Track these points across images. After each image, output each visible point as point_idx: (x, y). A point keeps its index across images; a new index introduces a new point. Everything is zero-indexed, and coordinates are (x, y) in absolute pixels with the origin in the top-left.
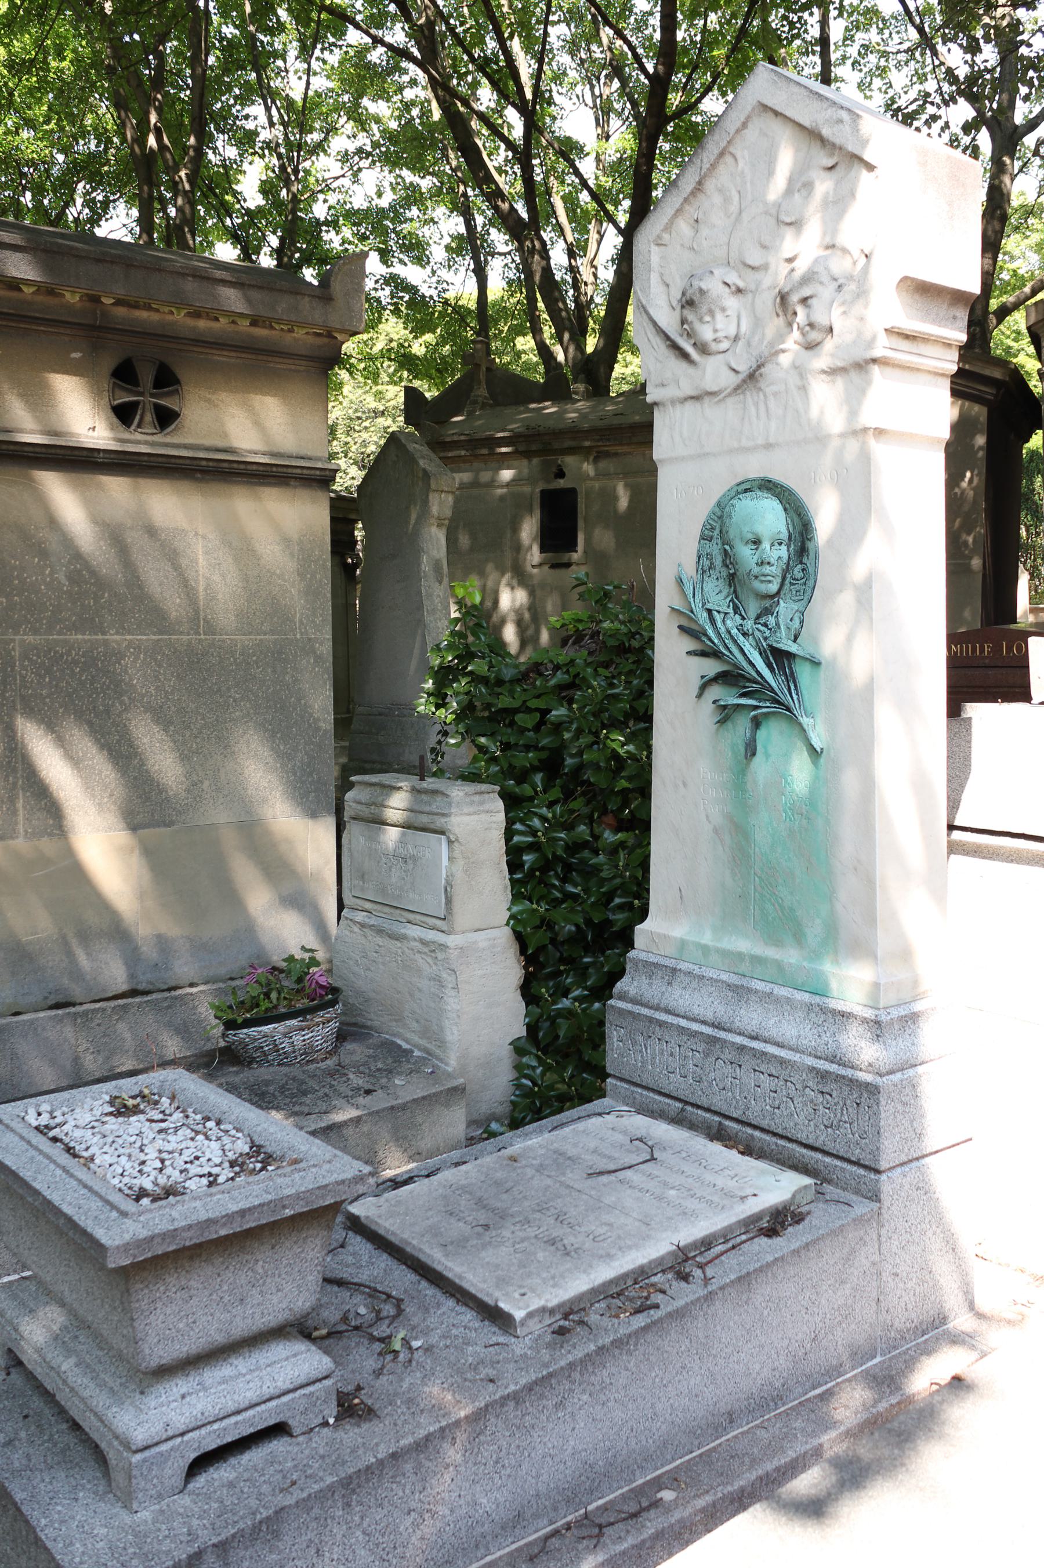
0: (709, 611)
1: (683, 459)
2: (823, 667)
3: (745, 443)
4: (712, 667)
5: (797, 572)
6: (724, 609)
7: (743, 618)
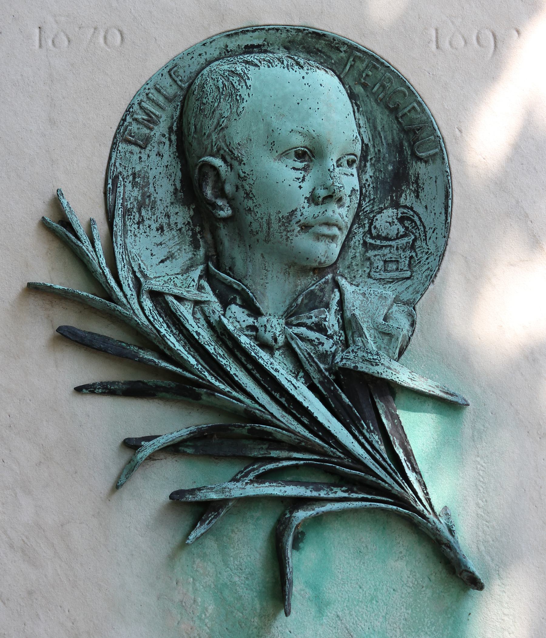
0: (156, 296)
2: (468, 414)
4: (167, 422)
5: (386, 220)
6: (193, 294)
7: (256, 312)
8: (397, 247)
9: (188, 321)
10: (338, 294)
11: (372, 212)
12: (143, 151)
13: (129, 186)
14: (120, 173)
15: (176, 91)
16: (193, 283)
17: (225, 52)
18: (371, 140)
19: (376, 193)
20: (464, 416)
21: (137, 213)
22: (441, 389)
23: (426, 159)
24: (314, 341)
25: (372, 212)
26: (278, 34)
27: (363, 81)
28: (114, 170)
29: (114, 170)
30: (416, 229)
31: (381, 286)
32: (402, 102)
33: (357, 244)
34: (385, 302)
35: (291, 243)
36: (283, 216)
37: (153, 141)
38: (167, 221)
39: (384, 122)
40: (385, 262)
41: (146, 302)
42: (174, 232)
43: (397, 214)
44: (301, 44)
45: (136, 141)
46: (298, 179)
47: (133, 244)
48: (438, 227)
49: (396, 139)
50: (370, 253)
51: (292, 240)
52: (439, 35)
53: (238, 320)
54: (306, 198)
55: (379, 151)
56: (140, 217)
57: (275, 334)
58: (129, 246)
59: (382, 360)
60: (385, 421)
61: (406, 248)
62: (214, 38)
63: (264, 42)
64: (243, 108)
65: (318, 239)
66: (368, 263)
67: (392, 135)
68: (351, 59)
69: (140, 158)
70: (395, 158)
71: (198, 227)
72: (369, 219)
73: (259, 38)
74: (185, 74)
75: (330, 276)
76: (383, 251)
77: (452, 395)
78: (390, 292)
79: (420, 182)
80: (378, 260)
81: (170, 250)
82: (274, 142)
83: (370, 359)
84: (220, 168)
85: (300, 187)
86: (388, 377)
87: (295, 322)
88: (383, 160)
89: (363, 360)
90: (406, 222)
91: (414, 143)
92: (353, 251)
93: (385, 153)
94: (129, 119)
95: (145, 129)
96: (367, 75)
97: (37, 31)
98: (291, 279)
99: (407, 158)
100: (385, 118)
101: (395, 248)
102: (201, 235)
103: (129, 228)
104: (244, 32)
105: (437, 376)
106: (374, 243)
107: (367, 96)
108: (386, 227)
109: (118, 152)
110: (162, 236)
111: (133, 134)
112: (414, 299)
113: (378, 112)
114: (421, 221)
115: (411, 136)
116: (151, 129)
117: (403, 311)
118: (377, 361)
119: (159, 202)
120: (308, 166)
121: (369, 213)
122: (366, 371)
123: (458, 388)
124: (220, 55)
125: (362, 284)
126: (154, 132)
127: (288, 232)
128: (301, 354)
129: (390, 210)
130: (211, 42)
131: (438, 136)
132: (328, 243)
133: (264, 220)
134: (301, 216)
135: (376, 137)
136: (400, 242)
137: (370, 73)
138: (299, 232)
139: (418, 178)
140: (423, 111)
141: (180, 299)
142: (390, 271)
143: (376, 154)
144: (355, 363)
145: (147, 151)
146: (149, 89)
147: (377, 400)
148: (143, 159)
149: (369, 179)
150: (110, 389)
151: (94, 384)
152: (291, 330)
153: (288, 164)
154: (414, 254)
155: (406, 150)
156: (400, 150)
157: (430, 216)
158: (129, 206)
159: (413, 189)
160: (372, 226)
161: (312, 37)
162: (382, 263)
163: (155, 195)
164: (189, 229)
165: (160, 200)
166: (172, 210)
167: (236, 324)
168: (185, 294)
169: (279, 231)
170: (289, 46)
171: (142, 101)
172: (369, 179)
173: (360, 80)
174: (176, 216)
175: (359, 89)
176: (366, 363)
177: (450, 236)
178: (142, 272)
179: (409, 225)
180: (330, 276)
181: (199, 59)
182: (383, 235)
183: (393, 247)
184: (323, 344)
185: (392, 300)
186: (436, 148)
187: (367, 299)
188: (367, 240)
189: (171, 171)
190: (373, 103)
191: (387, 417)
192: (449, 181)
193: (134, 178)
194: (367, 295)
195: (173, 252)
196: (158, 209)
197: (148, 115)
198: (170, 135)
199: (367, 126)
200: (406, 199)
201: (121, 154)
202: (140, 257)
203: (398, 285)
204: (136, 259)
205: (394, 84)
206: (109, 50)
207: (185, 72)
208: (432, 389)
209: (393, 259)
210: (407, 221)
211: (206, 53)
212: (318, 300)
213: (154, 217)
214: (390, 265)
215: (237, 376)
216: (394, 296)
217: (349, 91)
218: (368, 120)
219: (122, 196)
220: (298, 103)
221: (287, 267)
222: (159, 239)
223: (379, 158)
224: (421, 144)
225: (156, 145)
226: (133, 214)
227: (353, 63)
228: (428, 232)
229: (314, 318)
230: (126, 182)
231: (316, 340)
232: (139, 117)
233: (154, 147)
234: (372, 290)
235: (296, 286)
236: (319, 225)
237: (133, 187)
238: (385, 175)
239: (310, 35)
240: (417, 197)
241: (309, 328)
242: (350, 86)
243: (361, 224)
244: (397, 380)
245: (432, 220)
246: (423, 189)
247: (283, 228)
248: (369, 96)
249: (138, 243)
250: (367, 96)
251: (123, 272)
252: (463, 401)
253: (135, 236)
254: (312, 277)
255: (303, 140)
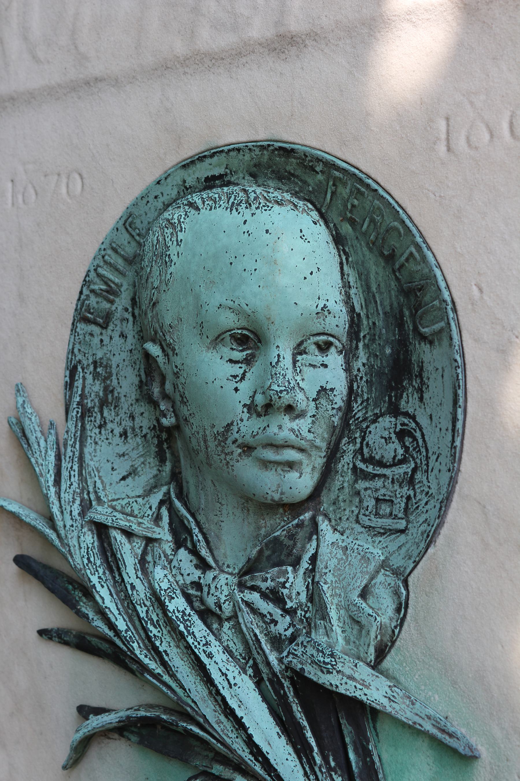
1: (30, 98)
3: (208, 39)
5: (381, 435)
6: (144, 526)
7: (203, 565)
8: (393, 479)
9: (126, 567)
10: (314, 543)
11: (365, 419)
12: (104, 331)
13: (90, 378)
14: (80, 362)
15: (135, 249)
16: (150, 512)
17: (183, 191)
18: (364, 306)
19: (370, 391)
20: (475, 770)
21: (99, 414)
22: (434, 723)
23: (430, 338)
24: (265, 616)
25: (365, 419)
26: (241, 157)
27: (349, 215)
28: (72, 359)
29: (72, 359)
30: (417, 452)
31: (369, 538)
32: (397, 245)
33: (345, 469)
34: (367, 567)
35: (233, 470)
36: (218, 432)
37: (115, 318)
38: (132, 425)
39: (380, 279)
40: (377, 500)
41: (86, 536)
42: (139, 440)
43: (396, 425)
44: (270, 167)
45: (95, 319)
46: (235, 377)
47: (93, 454)
48: (443, 454)
49: (395, 304)
50: (361, 485)
51: (233, 466)
52: (451, 128)
53: (183, 571)
54: (245, 405)
55: (374, 324)
56: (101, 419)
57: (219, 599)
58: (87, 457)
59: (340, 665)
60: (352, 756)
61: (403, 481)
62: (169, 172)
63: (227, 170)
64: (171, 274)
65: (266, 467)
66: (357, 500)
67: (390, 298)
68: (331, 183)
69: (102, 341)
70: (394, 335)
71: (164, 433)
72: (361, 431)
73: (219, 165)
74: (142, 225)
75: (307, 515)
76: (374, 484)
77: (451, 735)
78: (377, 552)
79: (425, 375)
80: (369, 496)
81: (133, 463)
82: (202, 323)
83: (320, 661)
84: (157, 359)
85: (236, 390)
86: (348, 693)
87: (249, 584)
88: (380, 338)
89: (312, 662)
90: (407, 438)
91: (416, 312)
92: (341, 479)
93: (381, 327)
94: (86, 292)
95: (105, 302)
96: (353, 206)
97: (10, 185)
98: (252, 518)
99: (409, 335)
100: (380, 271)
101: (390, 480)
102: (167, 444)
103: (89, 433)
104: (201, 158)
105: (437, 697)
106: (366, 469)
107: (357, 238)
108: (381, 446)
109: (76, 334)
110: (125, 444)
111: (92, 311)
112: (405, 568)
113: (371, 262)
114: (424, 440)
115: (413, 300)
116: (112, 302)
117: (389, 584)
118: (329, 666)
119: (123, 399)
120: (253, 356)
121: (361, 422)
122: (315, 679)
123: (468, 723)
124: (179, 195)
125: (348, 532)
126: (116, 305)
127: (226, 454)
128: (247, 634)
129: (387, 419)
130: (166, 179)
131: (444, 301)
132: (282, 473)
133: (200, 436)
134: (237, 432)
135: (370, 302)
136: (397, 472)
137: (356, 202)
138: (240, 455)
139: (421, 369)
140: (424, 258)
141: (129, 534)
142: (382, 517)
143: (370, 328)
144: (302, 664)
145: (109, 332)
146: (105, 250)
147: (343, 721)
148: (105, 343)
149: (362, 368)
150: (64, 640)
151: (52, 630)
152: (242, 595)
153: (223, 355)
154: (411, 493)
155: (407, 322)
156: (401, 325)
157: (435, 432)
158: (89, 405)
159: (416, 386)
160: (365, 443)
161: (279, 156)
162: (373, 502)
163: (119, 390)
164: (154, 436)
165: (125, 396)
166: (138, 409)
167: (179, 578)
168: (134, 527)
169: (217, 453)
170: (255, 174)
171: (98, 266)
172: (362, 368)
173: (346, 214)
174: (140, 417)
175: (346, 229)
176: (314, 666)
177: (461, 469)
178: (96, 492)
179: (410, 443)
180: (307, 515)
181: (155, 203)
182: (377, 457)
183: (388, 478)
184: (276, 623)
185: (378, 564)
186: (442, 319)
187: (347, 558)
188: (357, 464)
189: (136, 357)
190: (365, 249)
191: (356, 751)
192: (458, 376)
193: (95, 368)
194: (348, 552)
195: (136, 466)
196: (122, 409)
197: (106, 283)
198: (133, 309)
199: (359, 285)
200: (408, 402)
201: (80, 337)
202: (99, 472)
203: (390, 541)
204: (93, 475)
205: (386, 218)
206: (69, 201)
207: (142, 222)
208: (420, 721)
209: (387, 498)
210: (409, 437)
211: (162, 194)
212: (285, 552)
213: (117, 419)
214: (383, 506)
215: (167, 655)
216: (382, 558)
217: (334, 233)
218: (360, 275)
219: (80, 392)
220: (231, 263)
221: (243, 501)
222: (122, 449)
223: (375, 335)
224: (424, 313)
225: (118, 322)
226: (94, 415)
227: (333, 188)
228: (431, 459)
229: (269, 580)
230: (86, 373)
231: (268, 616)
232: (96, 287)
233: (116, 325)
234: (358, 542)
235: (259, 528)
236: (263, 447)
237: (94, 380)
238: (381, 363)
239: (276, 152)
240: (421, 399)
241: (264, 596)
242: (335, 225)
243: (351, 437)
244: (364, 698)
245: (436, 439)
246: (428, 386)
247: (220, 448)
248: (359, 238)
249: (98, 453)
250: (357, 238)
251: (67, 494)
252: (467, 749)
253: (96, 443)
254: (282, 515)
255: (236, 319)
